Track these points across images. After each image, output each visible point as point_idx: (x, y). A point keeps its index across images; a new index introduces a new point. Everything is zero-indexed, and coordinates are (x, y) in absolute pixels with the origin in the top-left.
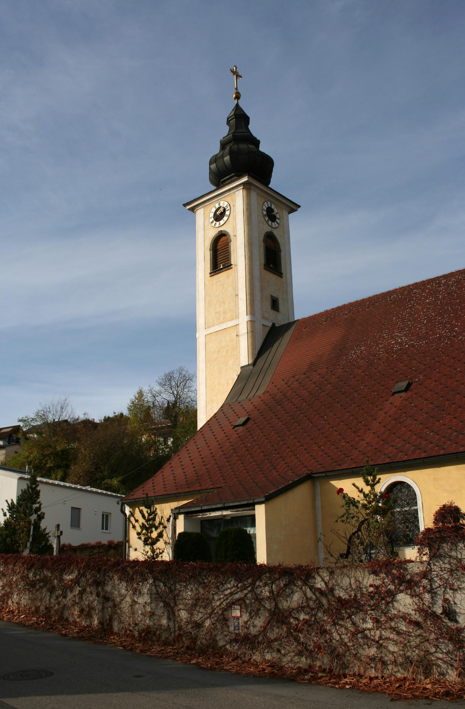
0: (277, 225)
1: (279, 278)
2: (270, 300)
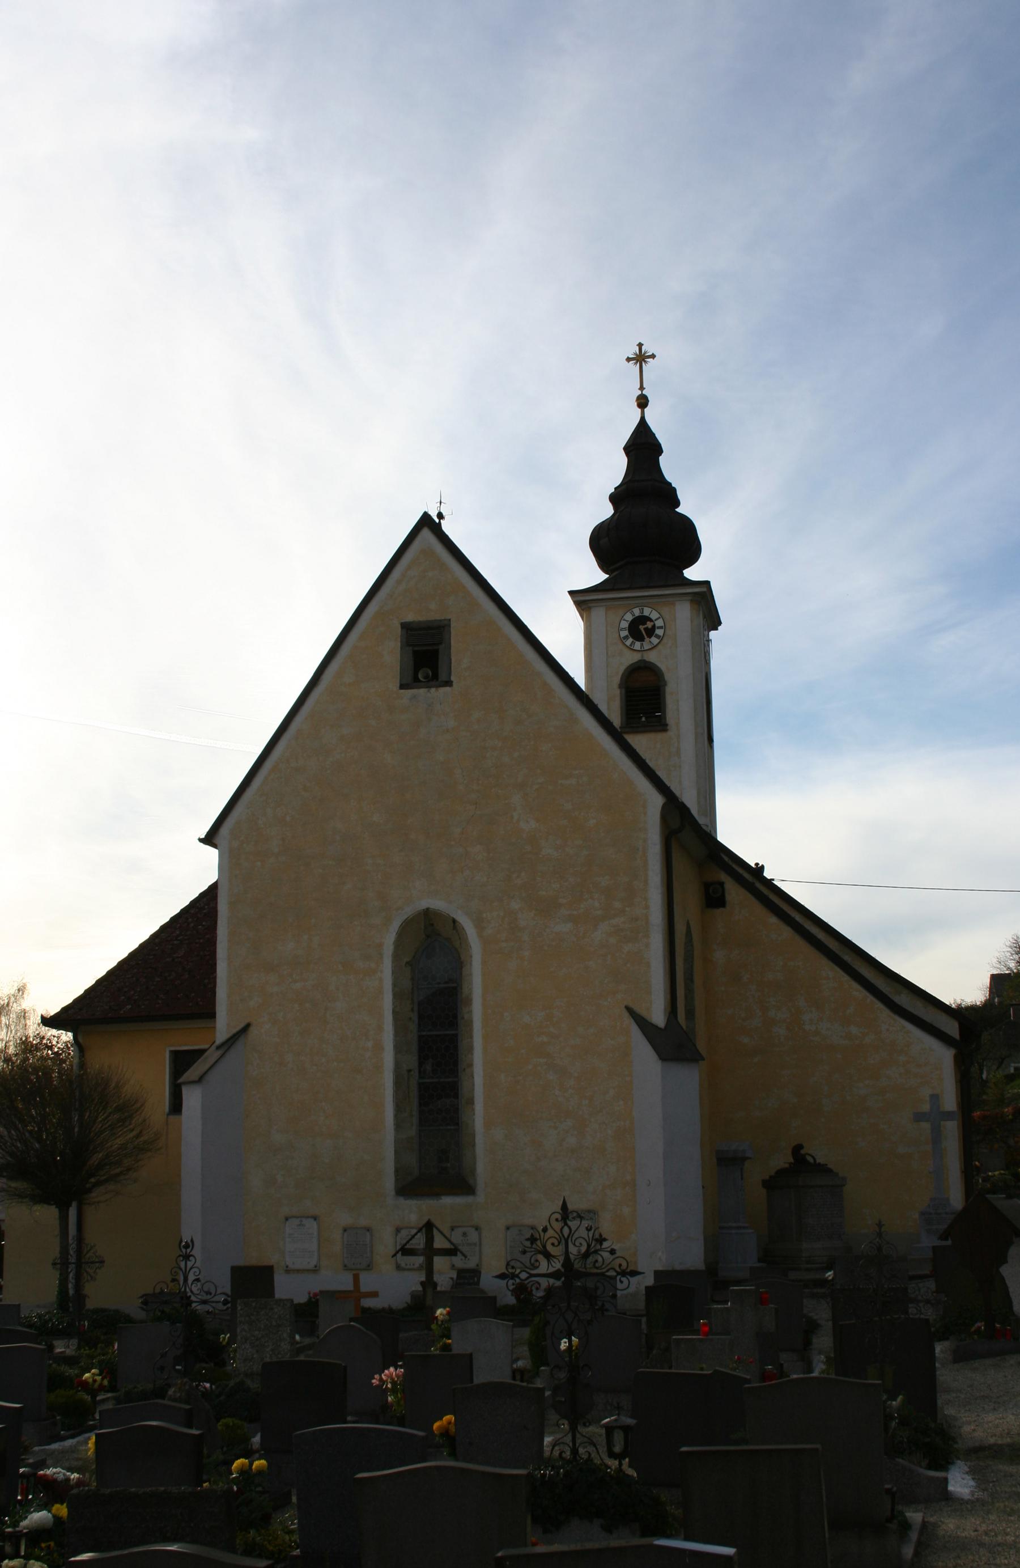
0: (658, 641)
1: (659, 736)
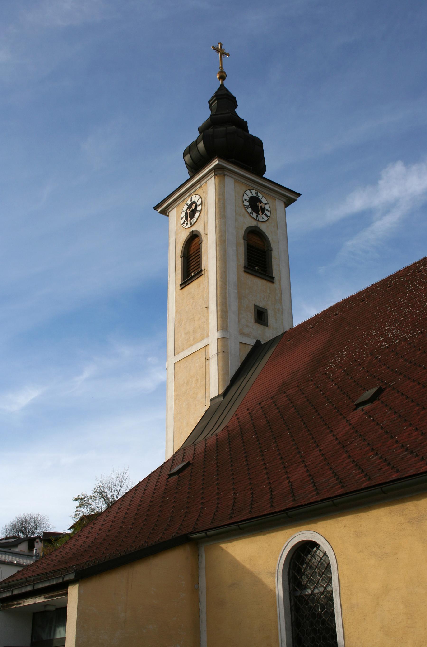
0: (266, 219)
1: (269, 284)
2: (253, 311)
